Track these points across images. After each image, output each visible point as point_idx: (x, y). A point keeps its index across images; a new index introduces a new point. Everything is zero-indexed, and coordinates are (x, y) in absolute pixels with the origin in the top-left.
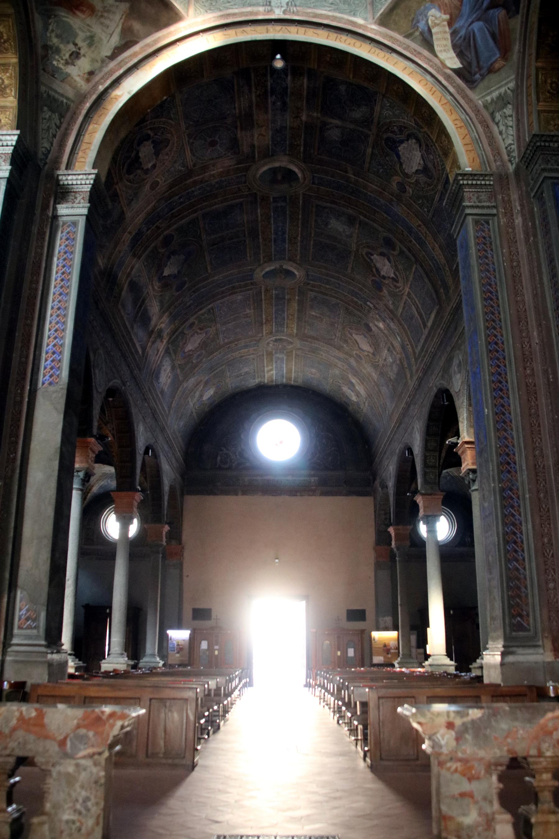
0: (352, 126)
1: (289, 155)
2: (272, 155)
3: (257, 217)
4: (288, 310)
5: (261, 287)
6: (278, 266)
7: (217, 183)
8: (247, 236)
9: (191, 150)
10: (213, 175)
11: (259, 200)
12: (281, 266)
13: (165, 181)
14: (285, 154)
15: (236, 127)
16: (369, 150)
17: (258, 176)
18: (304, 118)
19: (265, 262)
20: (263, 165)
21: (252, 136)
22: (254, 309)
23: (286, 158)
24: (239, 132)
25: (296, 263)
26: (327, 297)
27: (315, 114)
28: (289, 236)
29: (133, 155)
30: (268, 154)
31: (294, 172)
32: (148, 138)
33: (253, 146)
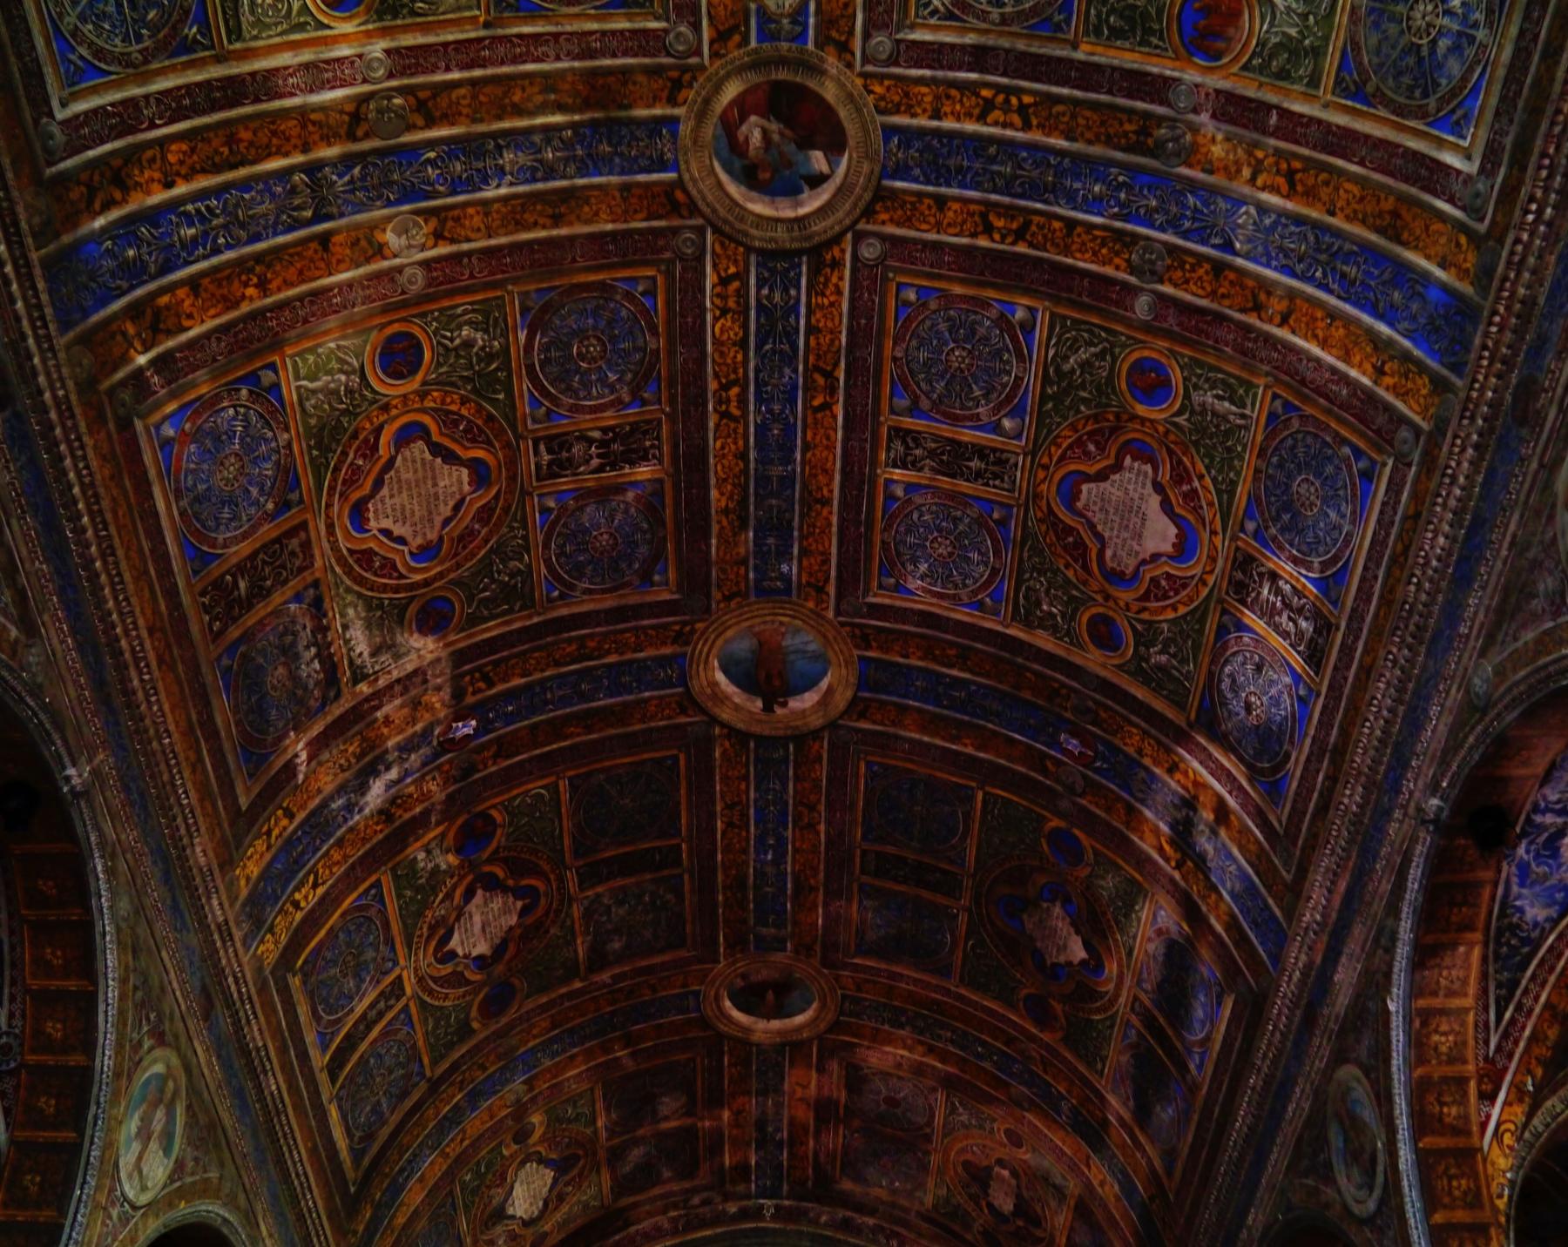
0: (640, 1132)
1: (751, 1045)
2: (783, 1045)
3: (826, 905)
4: (743, 456)
5: (838, 613)
6: (779, 711)
7: (901, 1026)
8: (858, 852)
9: (933, 1116)
10: (905, 1047)
11: (818, 948)
12: (768, 708)
13: (994, 1120)
14: (758, 1045)
15: (846, 1107)
16: (600, 1123)
17: (815, 1005)
18: (726, 1114)
19: (816, 734)
20: (800, 1028)
21: (820, 1087)
22: (873, 478)
23: (755, 1038)
24: (843, 1100)
25: (723, 725)
26: (609, 602)
27: (707, 1124)
28: (748, 832)
29: (1020, 1223)
30: (793, 1048)
31: (740, 1009)
32: (990, 1206)
33: (821, 1070)
